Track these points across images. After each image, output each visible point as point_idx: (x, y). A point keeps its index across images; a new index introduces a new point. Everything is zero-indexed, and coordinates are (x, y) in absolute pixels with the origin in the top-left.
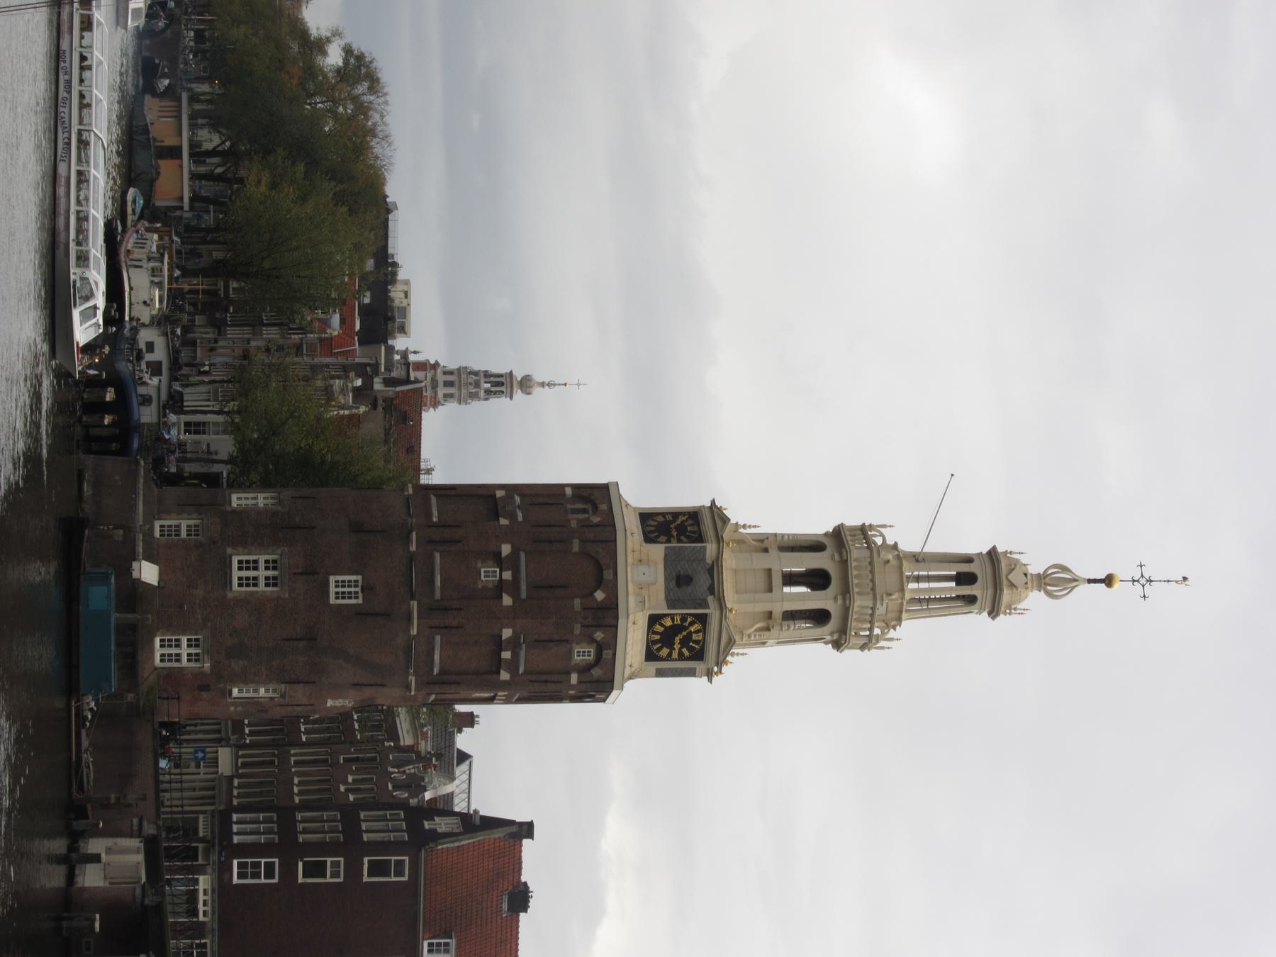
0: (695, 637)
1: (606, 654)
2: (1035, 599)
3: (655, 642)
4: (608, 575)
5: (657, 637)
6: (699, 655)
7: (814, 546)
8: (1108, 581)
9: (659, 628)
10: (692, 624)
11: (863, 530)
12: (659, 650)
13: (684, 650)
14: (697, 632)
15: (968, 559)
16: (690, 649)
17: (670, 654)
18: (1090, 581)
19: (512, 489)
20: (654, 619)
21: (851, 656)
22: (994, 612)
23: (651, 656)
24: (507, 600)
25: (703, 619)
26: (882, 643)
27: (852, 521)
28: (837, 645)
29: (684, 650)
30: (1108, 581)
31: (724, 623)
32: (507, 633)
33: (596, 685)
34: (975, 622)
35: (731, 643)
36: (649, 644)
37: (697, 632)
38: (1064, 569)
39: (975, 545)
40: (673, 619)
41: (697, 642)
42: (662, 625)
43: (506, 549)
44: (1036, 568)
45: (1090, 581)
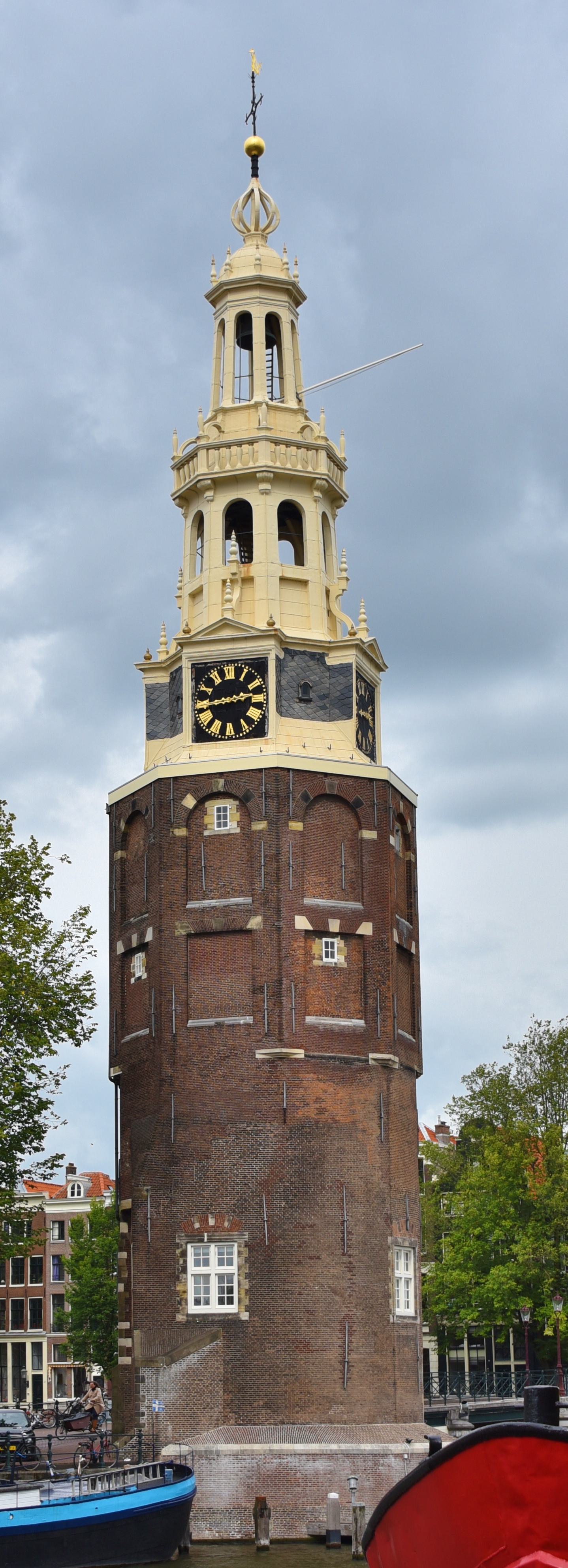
0: (230, 675)
3: (238, 729)
5: (230, 727)
6: (259, 666)
9: (218, 724)
10: (210, 682)
12: (249, 721)
13: (251, 687)
14: (222, 674)
16: (250, 678)
17: (259, 705)
18: (255, 174)
20: (201, 735)
23: (259, 730)
24: (149, 937)
25: (201, 672)
29: (251, 687)
30: (255, 153)
31: (199, 638)
35: (225, 624)
36: (238, 734)
37: (222, 674)
40: (202, 711)
41: (238, 671)
42: (211, 723)
45: (255, 174)
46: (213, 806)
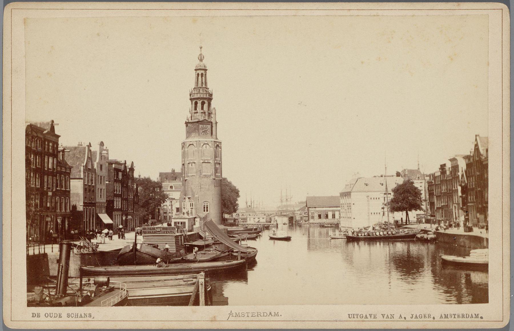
1: (206, 143)
8: (201, 48)
11: (190, 95)
21: (213, 96)
22: (206, 70)
30: (201, 48)
39: (194, 75)
46: (205, 145)
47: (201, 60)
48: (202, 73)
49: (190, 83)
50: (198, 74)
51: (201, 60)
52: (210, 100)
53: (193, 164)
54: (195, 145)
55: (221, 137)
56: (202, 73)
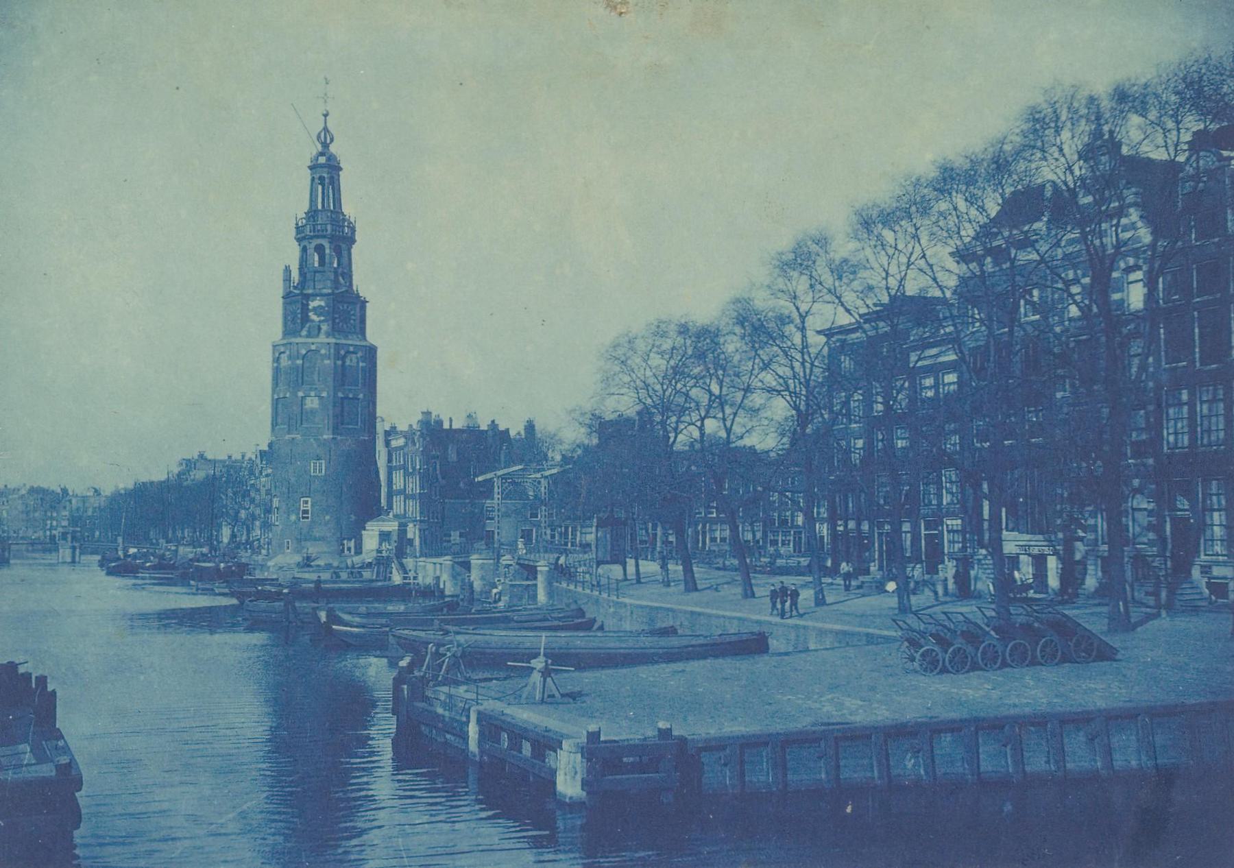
1: (351, 349)
2: (333, 149)
4: (313, 347)
7: (304, 250)
8: (326, 116)
11: (297, 228)
15: (313, 179)
19: (274, 391)
22: (341, 169)
26: (352, 220)
27: (294, 232)
28: (353, 241)
30: (326, 116)
32: (340, 395)
33: (371, 353)
34: (345, 179)
38: (319, 137)
39: (307, 174)
43: (300, 394)
44: (320, 148)
47: (325, 145)
48: (326, 172)
49: (296, 199)
50: (321, 179)
51: (325, 145)
52: (351, 240)
53: (316, 400)
54: (323, 351)
55: (372, 336)
56: (326, 172)
